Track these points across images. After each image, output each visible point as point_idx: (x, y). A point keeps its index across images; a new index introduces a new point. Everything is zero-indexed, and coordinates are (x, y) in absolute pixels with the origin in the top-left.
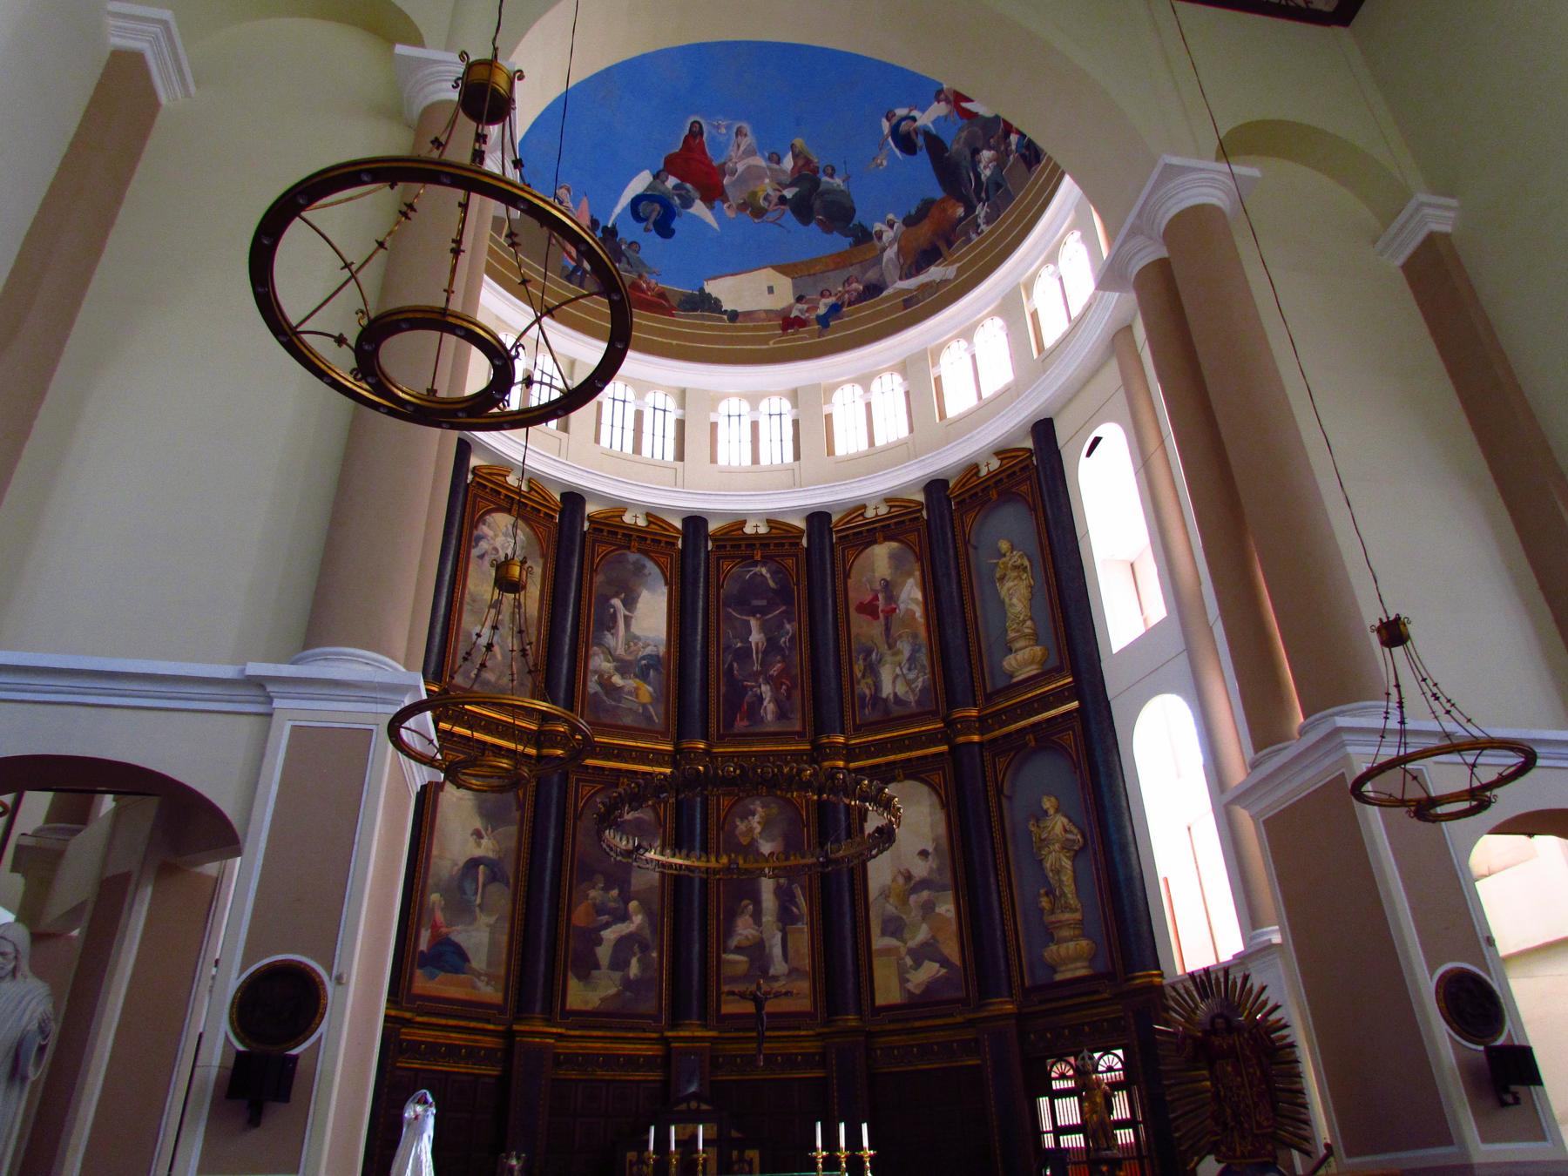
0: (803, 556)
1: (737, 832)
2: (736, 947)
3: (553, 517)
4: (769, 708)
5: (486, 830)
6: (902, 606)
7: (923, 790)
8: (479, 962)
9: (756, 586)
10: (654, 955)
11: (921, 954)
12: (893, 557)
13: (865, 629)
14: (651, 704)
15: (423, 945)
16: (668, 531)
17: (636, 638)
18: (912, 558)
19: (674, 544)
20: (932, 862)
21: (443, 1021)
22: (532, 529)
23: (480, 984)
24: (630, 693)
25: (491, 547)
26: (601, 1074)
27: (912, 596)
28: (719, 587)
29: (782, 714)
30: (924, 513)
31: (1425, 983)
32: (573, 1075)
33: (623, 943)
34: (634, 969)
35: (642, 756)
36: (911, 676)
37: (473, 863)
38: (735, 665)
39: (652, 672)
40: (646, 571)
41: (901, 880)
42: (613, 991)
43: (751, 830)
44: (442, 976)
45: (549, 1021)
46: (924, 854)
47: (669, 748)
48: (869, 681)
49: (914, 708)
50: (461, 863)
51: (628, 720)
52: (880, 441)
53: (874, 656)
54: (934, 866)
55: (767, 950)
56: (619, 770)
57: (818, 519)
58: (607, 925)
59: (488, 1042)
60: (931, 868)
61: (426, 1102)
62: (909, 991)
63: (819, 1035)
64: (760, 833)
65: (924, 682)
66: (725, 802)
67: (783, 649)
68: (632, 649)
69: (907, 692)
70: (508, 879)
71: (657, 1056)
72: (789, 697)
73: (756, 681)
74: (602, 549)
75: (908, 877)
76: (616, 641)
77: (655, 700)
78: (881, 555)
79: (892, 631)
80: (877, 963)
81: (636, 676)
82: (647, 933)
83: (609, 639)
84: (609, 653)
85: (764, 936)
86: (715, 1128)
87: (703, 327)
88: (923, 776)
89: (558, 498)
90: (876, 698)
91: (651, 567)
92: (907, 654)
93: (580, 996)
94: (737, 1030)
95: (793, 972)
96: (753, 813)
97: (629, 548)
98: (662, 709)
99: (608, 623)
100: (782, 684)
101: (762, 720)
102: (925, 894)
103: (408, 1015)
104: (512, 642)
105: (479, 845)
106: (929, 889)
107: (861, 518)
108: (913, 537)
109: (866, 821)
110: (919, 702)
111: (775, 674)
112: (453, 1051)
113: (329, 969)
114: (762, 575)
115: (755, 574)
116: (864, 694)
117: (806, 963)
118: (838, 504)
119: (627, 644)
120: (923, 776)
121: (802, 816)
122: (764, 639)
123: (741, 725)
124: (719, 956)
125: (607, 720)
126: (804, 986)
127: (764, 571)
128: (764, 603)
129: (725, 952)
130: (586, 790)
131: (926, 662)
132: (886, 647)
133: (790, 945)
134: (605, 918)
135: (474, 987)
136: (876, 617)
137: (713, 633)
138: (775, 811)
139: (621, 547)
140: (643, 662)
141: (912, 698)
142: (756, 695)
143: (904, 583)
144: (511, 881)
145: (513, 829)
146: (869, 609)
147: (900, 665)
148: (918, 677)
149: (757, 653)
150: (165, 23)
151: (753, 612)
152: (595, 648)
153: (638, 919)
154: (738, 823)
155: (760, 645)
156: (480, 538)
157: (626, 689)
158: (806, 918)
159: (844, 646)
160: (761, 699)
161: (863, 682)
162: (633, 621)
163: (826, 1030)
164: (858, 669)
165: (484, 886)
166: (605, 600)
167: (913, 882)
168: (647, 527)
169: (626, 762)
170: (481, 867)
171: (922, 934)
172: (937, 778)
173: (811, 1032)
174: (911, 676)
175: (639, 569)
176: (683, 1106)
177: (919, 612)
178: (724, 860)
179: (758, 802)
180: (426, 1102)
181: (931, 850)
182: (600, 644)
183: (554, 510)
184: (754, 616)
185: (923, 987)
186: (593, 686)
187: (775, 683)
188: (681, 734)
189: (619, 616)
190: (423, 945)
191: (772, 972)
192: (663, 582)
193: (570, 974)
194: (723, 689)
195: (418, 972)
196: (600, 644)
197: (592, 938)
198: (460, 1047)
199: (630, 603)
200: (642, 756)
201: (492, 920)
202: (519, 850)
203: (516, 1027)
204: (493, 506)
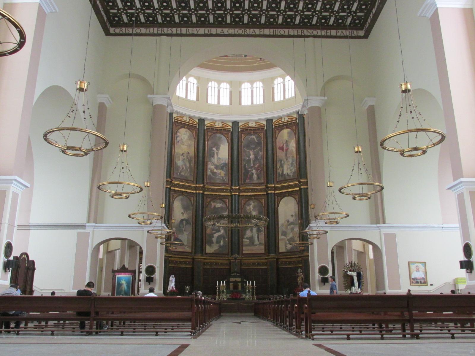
0: (264, 132)
1: (247, 209)
2: (246, 238)
3: (196, 127)
4: (255, 176)
5: (185, 212)
6: (290, 148)
7: (293, 199)
9: (251, 142)
10: (227, 240)
11: (291, 240)
12: (288, 133)
13: (280, 154)
14: (224, 176)
16: (227, 127)
17: (220, 158)
18: (293, 134)
20: (294, 218)
22: (191, 131)
23: (186, 248)
24: (219, 174)
25: (180, 139)
26: (215, 267)
27: (293, 145)
29: (258, 178)
30: (297, 120)
31: (317, 268)
32: (208, 267)
33: (219, 238)
34: (222, 243)
35: (222, 190)
36: (292, 168)
37: (182, 221)
38: (246, 165)
40: (222, 139)
41: (286, 222)
42: (217, 248)
43: (250, 209)
45: (202, 255)
46: (292, 216)
48: (281, 169)
49: (292, 177)
50: (179, 221)
51: (218, 181)
52: (287, 97)
53: (282, 162)
54: (295, 219)
55: (254, 239)
56: (216, 195)
57: (269, 121)
58: (215, 233)
59: (189, 260)
60: (294, 219)
61: (173, 277)
62: (287, 249)
63: (266, 259)
64: (252, 210)
65: (295, 170)
67: (259, 160)
68: (219, 162)
69: (290, 173)
70: (191, 224)
71: (228, 263)
72: (260, 173)
73: (252, 169)
75: (288, 221)
76: (215, 160)
77: (225, 175)
78: (285, 132)
79: (287, 155)
80: (280, 242)
81: (220, 169)
82: (225, 235)
83: (213, 160)
84: (213, 163)
85: (253, 235)
86: (240, 279)
87: (237, 60)
88: (293, 196)
89: (197, 121)
90: (282, 174)
91: (223, 138)
92: (291, 162)
94: (246, 257)
95: (260, 244)
96: (251, 205)
97: (217, 133)
98: (227, 178)
99: (212, 155)
100: (258, 169)
101: (253, 180)
102: (292, 226)
103: (170, 255)
105: (183, 216)
106: (293, 225)
107: (280, 121)
108: (294, 128)
109: (279, 207)
110: (293, 175)
111: (257, 167)
112: (181, 262)
113: (156, 266)
114: (253, 138)
115: (252, 138)
116: (280, 173)
117: (263, 242)
118: (275, 118)
119: (218, 161)
120: (293, 196)
121: (263, 205)
122: (254, 157)
123: (248, 181)
124: (242, 240)
125: (213, 181)
126: (263, 247)
127: (254, 137)
128: (254, 146)
129: (244, 238)
130: (208, 200)
131: (295, 165)
132: (286, 160)
133: (259, 237)
134: (214, 232)
135: (184, 248)
136: (283, 151)
138: (256, 204)
140: (222, 165)
141: (291, 174)
142: (251, 173)
143: (291, 141)
144: (191, 224)
145: (191, 212)
146: (282, 149)
147: (289, 165)
148: (293, 169)
149: (252, 161)
150: (107, 98)
151: (251, 150)
152: (209, 162)
153: (222, 231)
154: (247, 207)
155: (253, 159)
157: (218, 173)
158: (264, 231)
159: (275, 159)
160: (253, 174)
161: (279, 169)
162: (219, 154)
163: (266, 258)
164: (278, 166)
165: (185, 225)
167: (289, 223)
168: (222, 126)
169: (218, 192)
170: (184, 221)
171: (290, 236)
172: (296, 196)
173: (264, 258)
174: (292, 168)
175: (220, 138)
176: (233, 274)
177: (294, 150)
178: (235, 225)
179: (252, 202)
180: (173, 277)
181: (294, 215)
182: (210, 161)
183: (196, 125)
184: (251, 150)
185: (290, 248)
186: (209, 173)
187: (257, 170)
189: (215, 152)
191: (255, 244)
192: (227, 142)
194: (243, 171)
196: (210, 161)
199: (218, 149)
200: (222, 190)
201: (187, 233)
202: (193, 216)
203: (194, 257)
204: (180, 127)
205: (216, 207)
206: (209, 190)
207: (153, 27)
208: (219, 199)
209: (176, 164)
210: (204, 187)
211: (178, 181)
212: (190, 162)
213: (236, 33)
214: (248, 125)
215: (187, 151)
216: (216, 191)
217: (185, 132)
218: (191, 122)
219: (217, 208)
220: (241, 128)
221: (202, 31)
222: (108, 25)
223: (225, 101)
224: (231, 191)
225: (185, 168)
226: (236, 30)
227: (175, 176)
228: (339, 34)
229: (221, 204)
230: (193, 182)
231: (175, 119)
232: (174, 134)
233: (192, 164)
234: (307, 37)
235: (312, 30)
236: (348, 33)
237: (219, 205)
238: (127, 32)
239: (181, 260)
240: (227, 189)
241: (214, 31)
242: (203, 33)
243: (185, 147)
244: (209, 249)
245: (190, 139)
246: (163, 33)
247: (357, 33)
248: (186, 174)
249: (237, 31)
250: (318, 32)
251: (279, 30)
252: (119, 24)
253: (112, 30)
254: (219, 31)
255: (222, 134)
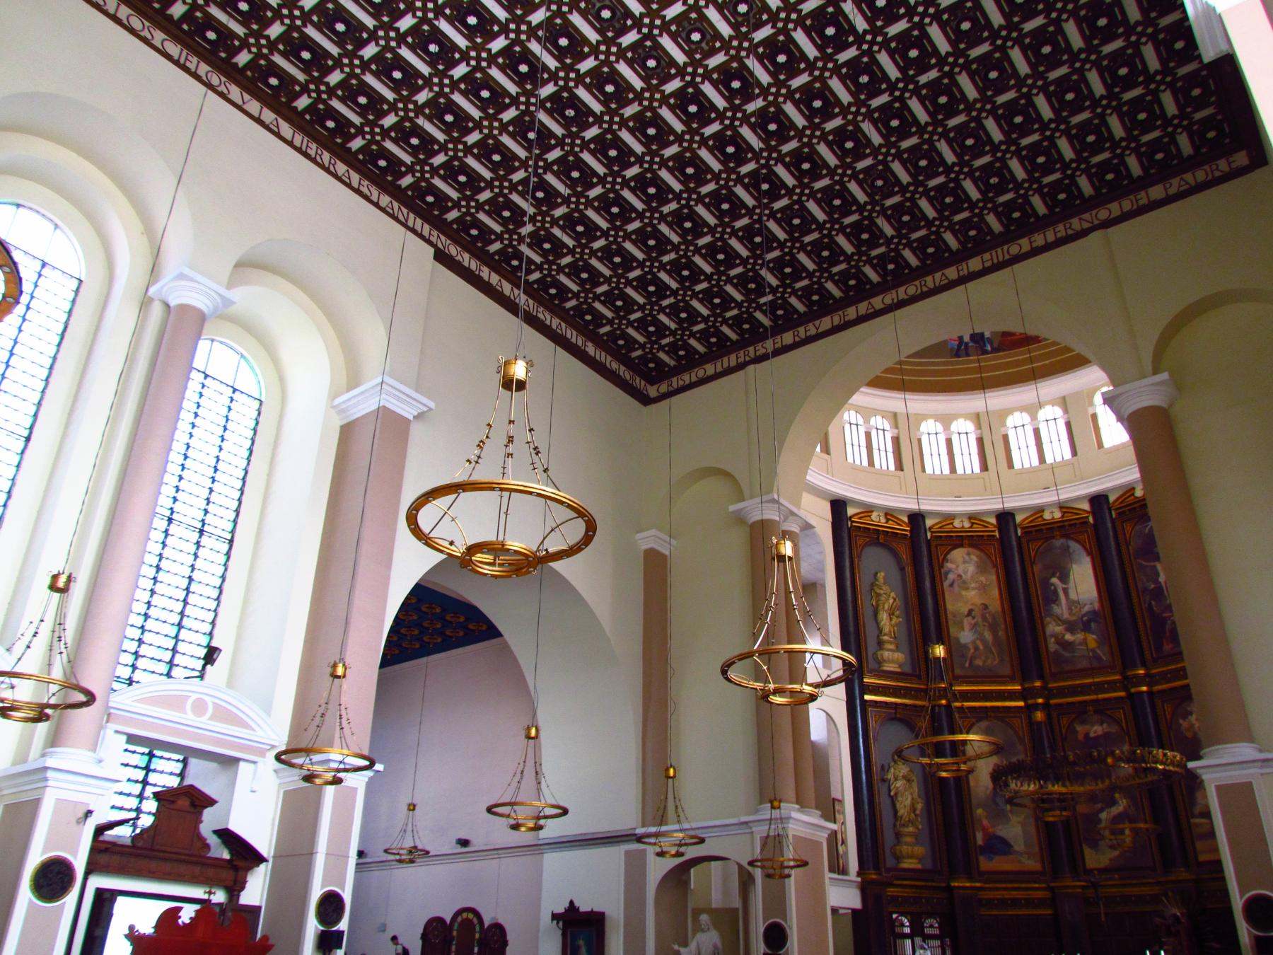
3: (994, 536)
8: (1019, 846)
14: (1098, 647)
15: (980, 841)
19: (1087, 522)
21: (1004, 885)
24: (1080, 644)
28: (1128, 544)
33: (1117, 819)
35: (1099, 688)
38: (1153, 603)
39: (1093, 625)
40: (1071, 550)
43: (1192, 726)
44: (997, 858)
47: (1117, 677)
51: (1084, 664)
56: (1085, 701)
58: (1101, 810)
59: (1040, 894)
66: (1168, 708)
74: (1033, 546)
76: (1062, 609)
81: (1082, 630)
83: (1056, 610)
84: (1059, 619)
91: (1074, 546)
93: (1096, 858)
96: (1191, 713)
99: (1052, 598)
104: (988, 636)
112: (1015, 903)
119: (1070, 609)
124: (1189, 823)
130: (1065, 721)
134: (1099, 805)
137: (1131, 581)
139: (1047, 539)
140: (1085, 619)
152: (1048, 619)
154: (1181, 721)
156: (947, 573)
157: (1077, 642)
166: (1046, 583)
168: (1062, 517)
175: (1066, 551)
178: (1107, 782)
182: (1050, 615)
186: (1053, 647)
188: (1126, 662)
190: (980, 841)
193: (1084, 845)
194: (1148, 624)
195: (981, 858)
196: (1050, 615)
197: (1093, 819)
198: (1021, 899)
199: (1064, 578)
200: (1099, 688)
201: (1021, 818)
205: (1092, 735)
206: (1062, 692)
207: (728, 353)
208: (1096, 712)
209: (957, 639)
210: (1044, 687)
211: (968, 683)
212: (993, 628)
213: (902, 296)
214: (1133, 494)
215: (979, 601)
216: (1083, 693)
217: (967, 557)
218: (976, 527)
219: (1096, 738)
220: (1116, 510)
221: (826, 323)
222: (639, 383)
223: (1058, 450)
224: (1127, 682)
225: (981, 647)
226: (901, 290)
227: (958, 671)
228: (1172, 191)
229: (1105, 725)
230: (1012, 680)
231: (932, 532)
232: (936, 568)
233: (1000, 633)
234: (1083, 233)
235: (1094, 212)
236: (1201, 175)
237: (1097, 730)
238: (681, 383)
239: (1015, 894)
240: (1114, 682)
241: (851, 313)
242: (829, 326)
243: (973, 593)
244: (1096, 858)
245: (981, 569)
246: (747, 359)
247: (1229, 164)
248: (989, 662)
249: (902, 293)
250: (1115, 209)
251: (1006, 247)
252: (659, 374)
253: (652, 391)
254: (863, 308)
255: (1067, 536)
